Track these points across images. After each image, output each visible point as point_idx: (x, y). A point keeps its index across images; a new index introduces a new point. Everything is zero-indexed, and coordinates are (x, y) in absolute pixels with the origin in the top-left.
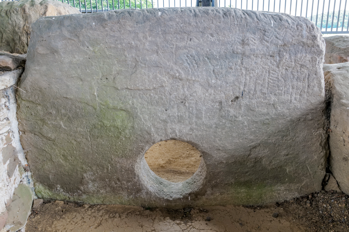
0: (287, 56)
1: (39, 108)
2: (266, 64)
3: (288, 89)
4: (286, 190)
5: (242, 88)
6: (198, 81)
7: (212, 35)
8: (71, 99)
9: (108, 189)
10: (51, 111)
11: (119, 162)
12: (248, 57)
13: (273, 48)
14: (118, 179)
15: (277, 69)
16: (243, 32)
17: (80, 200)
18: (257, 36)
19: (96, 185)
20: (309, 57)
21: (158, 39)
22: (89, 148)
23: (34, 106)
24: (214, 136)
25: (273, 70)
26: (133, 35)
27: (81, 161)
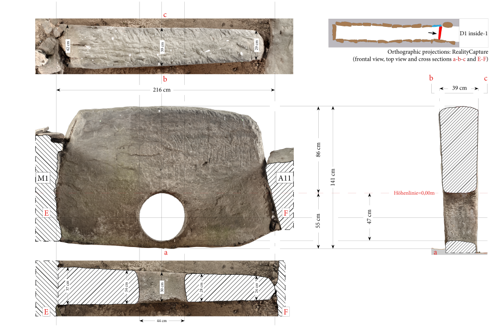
0: (236, 138)
1: (76, 166)
2: (223, 142)
3: (238, 158)
4: (245, 232)
5: (209, 156)
6: (181, 151)
7: (190, 124)
8: (99, 161)
9: (115, 231)
10: (84, 169)
11: (125, 208)
12: (212, 137)
13: (226, 133)
14: (123, 222)
15: (230, 145)
16: (208, 123)
17: (91, 241)
18: (216, 125)
19: (106, 227)
20: (249, 139)
21: (158, 125)
22: (105, 196)
23: (73, 165)
24: (192, 189)
25: (228, 146)
26: (143, 122)
27: (98, 207)
